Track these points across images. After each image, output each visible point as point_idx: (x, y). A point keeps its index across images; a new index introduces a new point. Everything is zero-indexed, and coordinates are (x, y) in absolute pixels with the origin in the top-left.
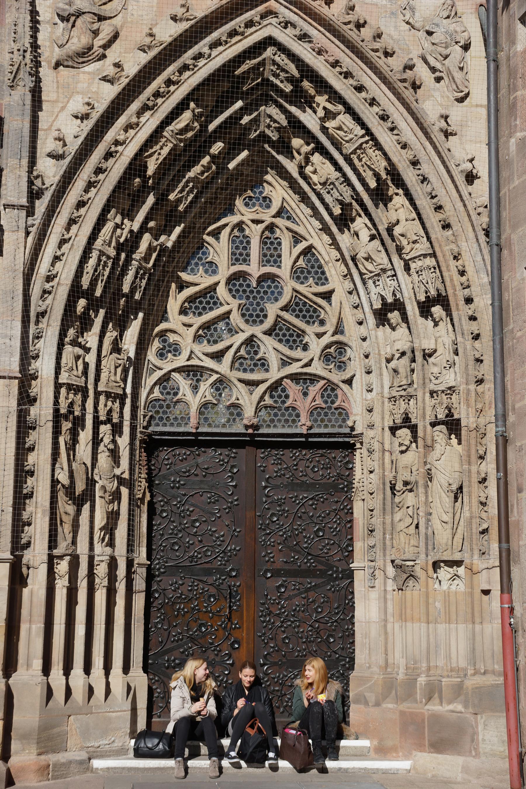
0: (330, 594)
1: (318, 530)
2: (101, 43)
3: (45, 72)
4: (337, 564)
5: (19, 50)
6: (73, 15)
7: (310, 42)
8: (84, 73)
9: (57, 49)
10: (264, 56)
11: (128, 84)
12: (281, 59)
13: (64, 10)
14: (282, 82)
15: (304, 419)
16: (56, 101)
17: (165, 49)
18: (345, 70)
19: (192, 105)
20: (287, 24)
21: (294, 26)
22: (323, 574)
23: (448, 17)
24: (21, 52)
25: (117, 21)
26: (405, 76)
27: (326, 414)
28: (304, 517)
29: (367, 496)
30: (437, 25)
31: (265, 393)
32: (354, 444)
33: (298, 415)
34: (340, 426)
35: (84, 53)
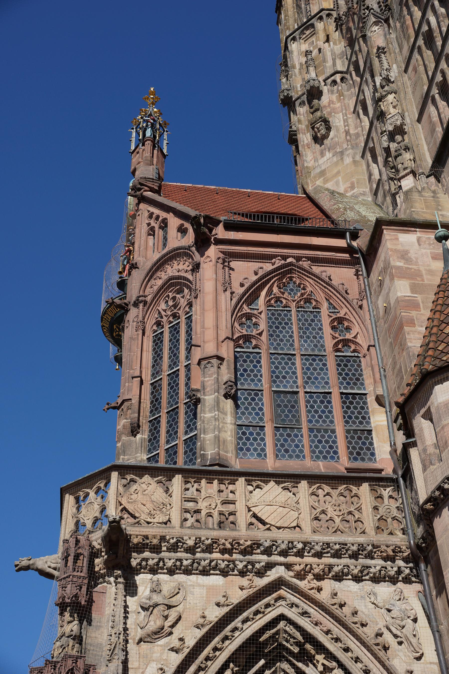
2: (170, 624)
3: (131, 646)
5: (115, 633)
6: (152, 606)
7: (310, 617)
8: (158, 646)
9: (139, 630)
10: (278, 627)
11: (189, 653)
12: (290, 629)
13: (146, 604)
14: (291, 645)
16: (139, 668)
17: (213, 626)
18: (335, 636)
19: (232, 665)
20: (292, 605)
21: (297, 606)
23: (400, 599)
24: (117, 635)
25: (180, 608)
26: (377, 641)
30: (394, 605)
35: (159, 632)
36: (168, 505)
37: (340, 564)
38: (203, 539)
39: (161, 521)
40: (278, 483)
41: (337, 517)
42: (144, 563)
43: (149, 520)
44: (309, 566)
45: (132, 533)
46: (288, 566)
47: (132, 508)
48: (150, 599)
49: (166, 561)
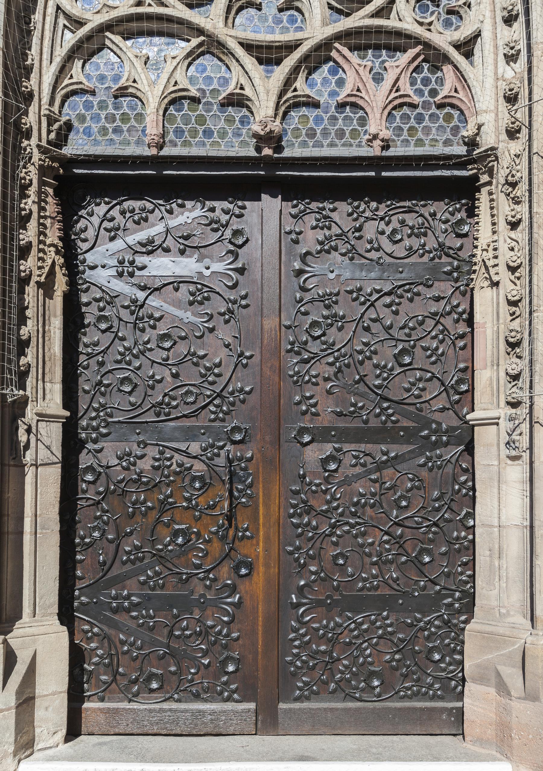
0: (424, 473)
1: (404, 352)
4: (437, 416)
15: (376, 124)
22: (410, 435)
27: (420, 118)
28: (376, 328)
31: (296, 70)
32: (475, 178)
33: (363, 122)
34: (447, 143)
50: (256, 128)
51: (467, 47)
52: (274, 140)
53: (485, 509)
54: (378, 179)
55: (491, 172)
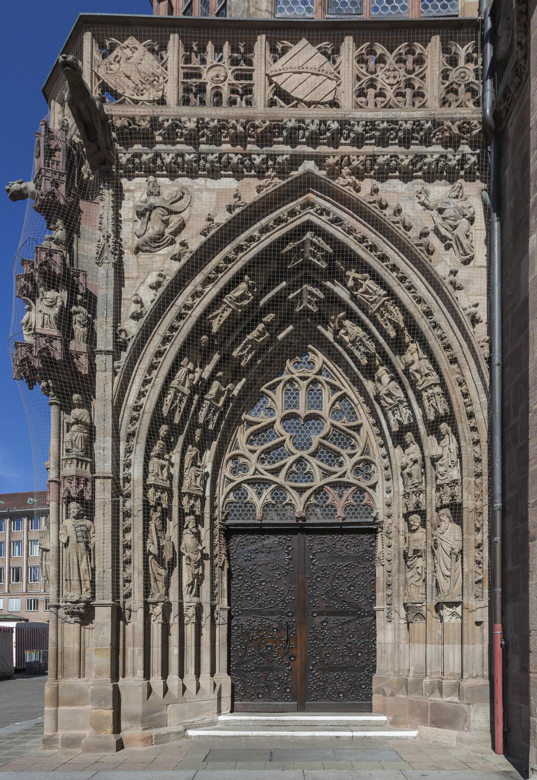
0: (359, 626)
1: (351, 586)
4: (364, 607)
7: (340, 225)
10: (304, 238)
13: (141, 206)
14: (319, 260)
15: (340, 513)
17: (221, 229)
19: (246, 277)
20: (323, 211)
21: (328, 214)
22: (354, 613)
23: (457, 197)
25: (185, 215)
27: (356, 510)
28: (340, 578)
29: (386, 563)
31: (311, 494)
32: (377, 529)
33: (335, 511)
34: (366, 517)
36: (161, 78)
37: (385, 154)
38: (207, 120)
39: (151, 99)
40: (313, 43)
41: (389, 87)
42: (137, 161)
43: (135, 97)
44: (346, 158)
45: (114, 113)
46: (320, 160)
47: (113, 81)
48: (146, 202)
49: (164, 155)
50: (296, 515)
51: (373, 487)
52: (304, 519)
53: (380, 638)
54: (341, 529)
55: (382, 528)
